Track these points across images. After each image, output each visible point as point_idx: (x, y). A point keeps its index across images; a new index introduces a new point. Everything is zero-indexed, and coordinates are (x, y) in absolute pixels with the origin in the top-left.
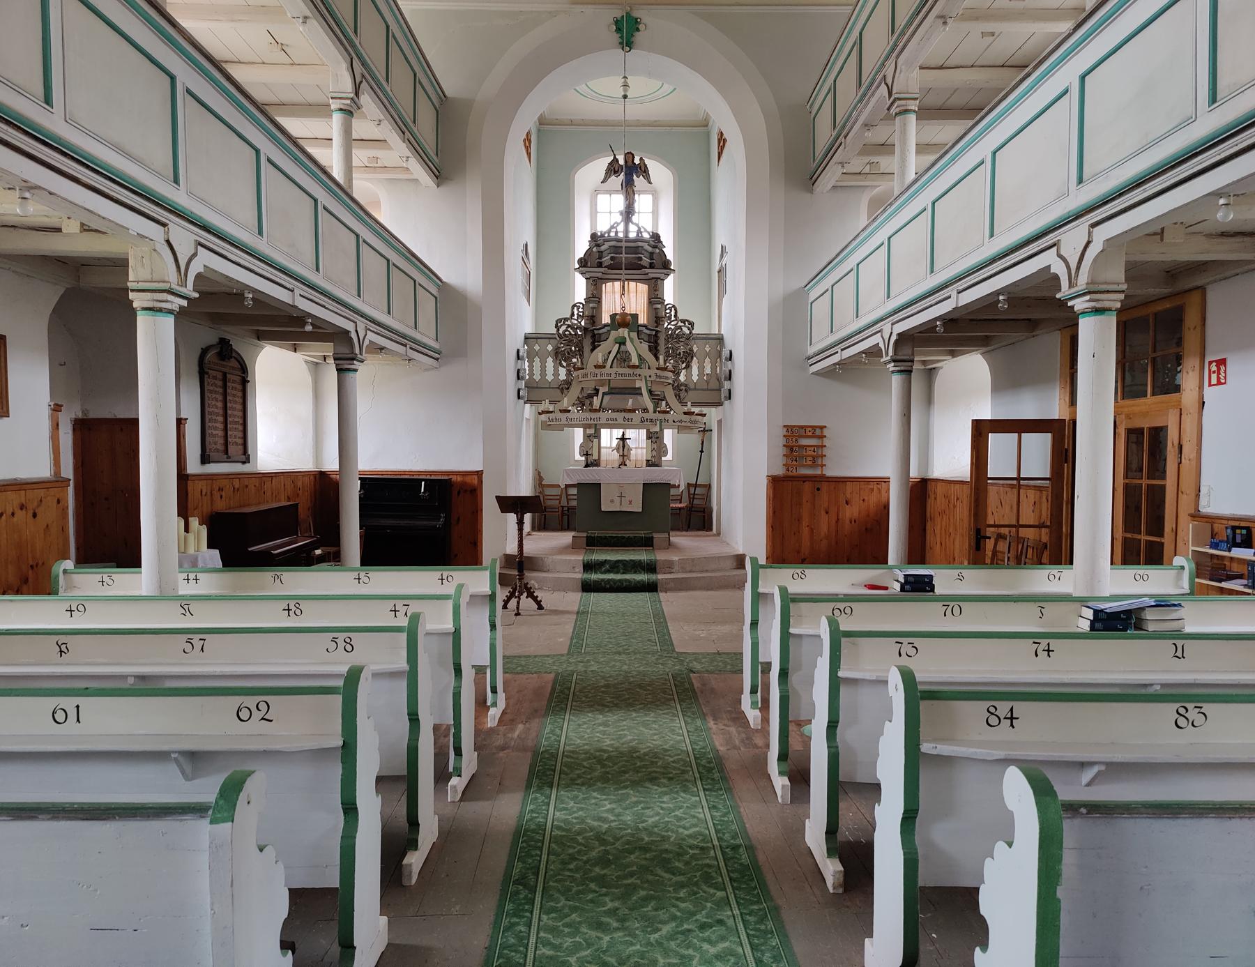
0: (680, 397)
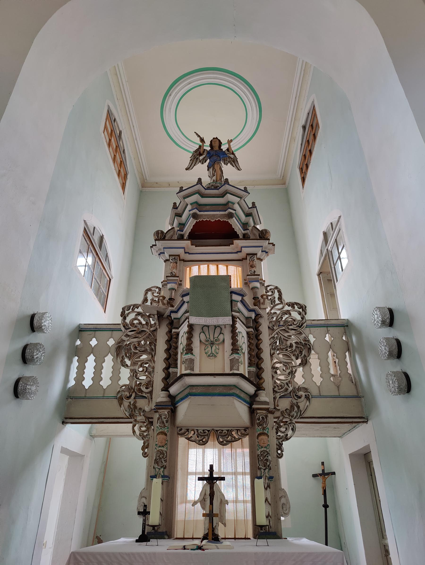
0: (298, 407)
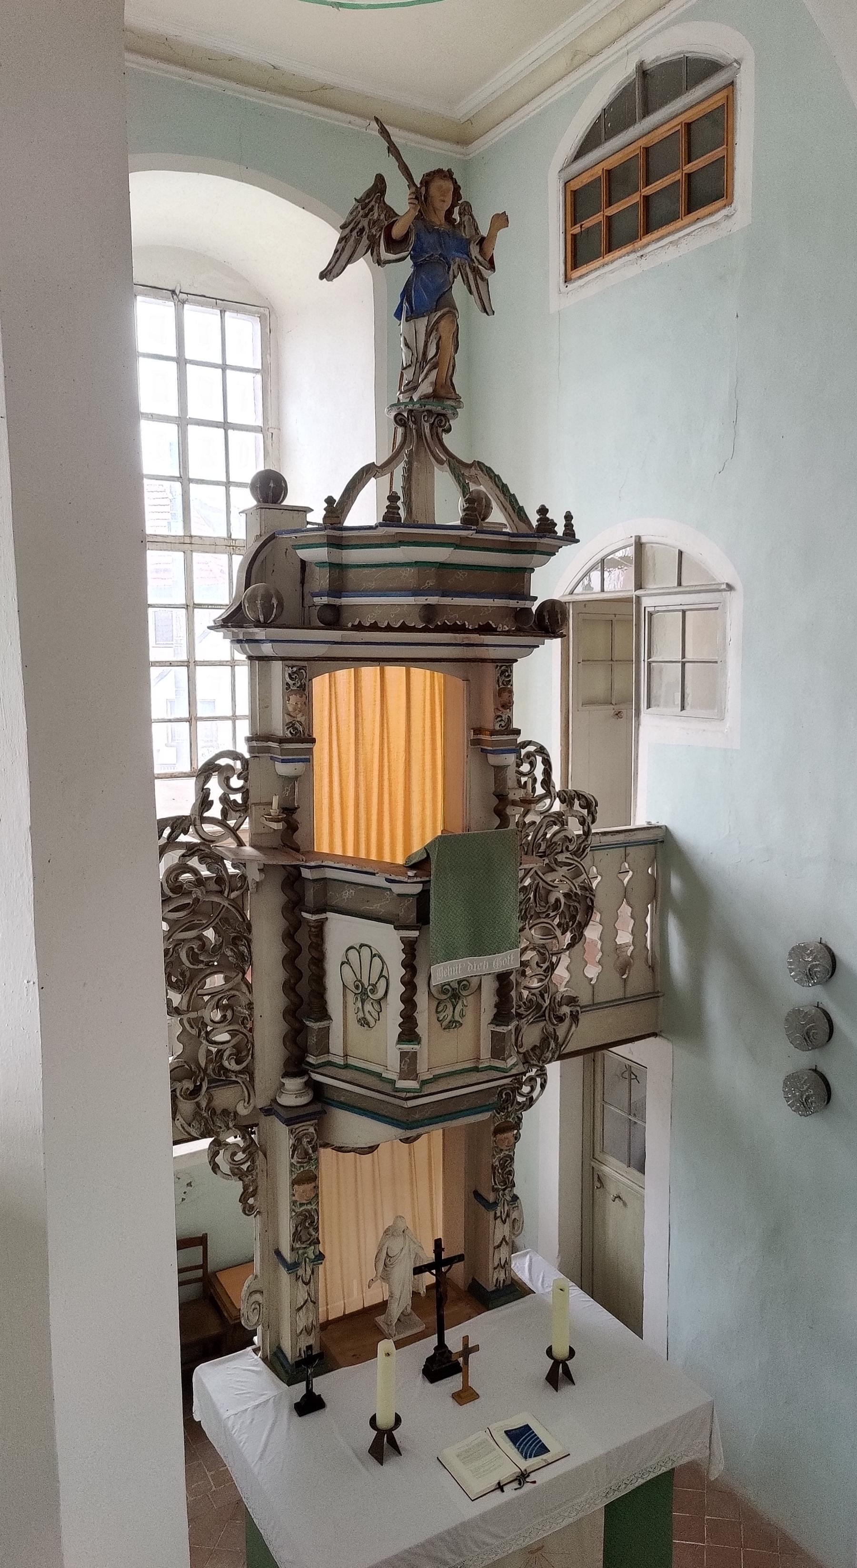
0: (556, 1038)
